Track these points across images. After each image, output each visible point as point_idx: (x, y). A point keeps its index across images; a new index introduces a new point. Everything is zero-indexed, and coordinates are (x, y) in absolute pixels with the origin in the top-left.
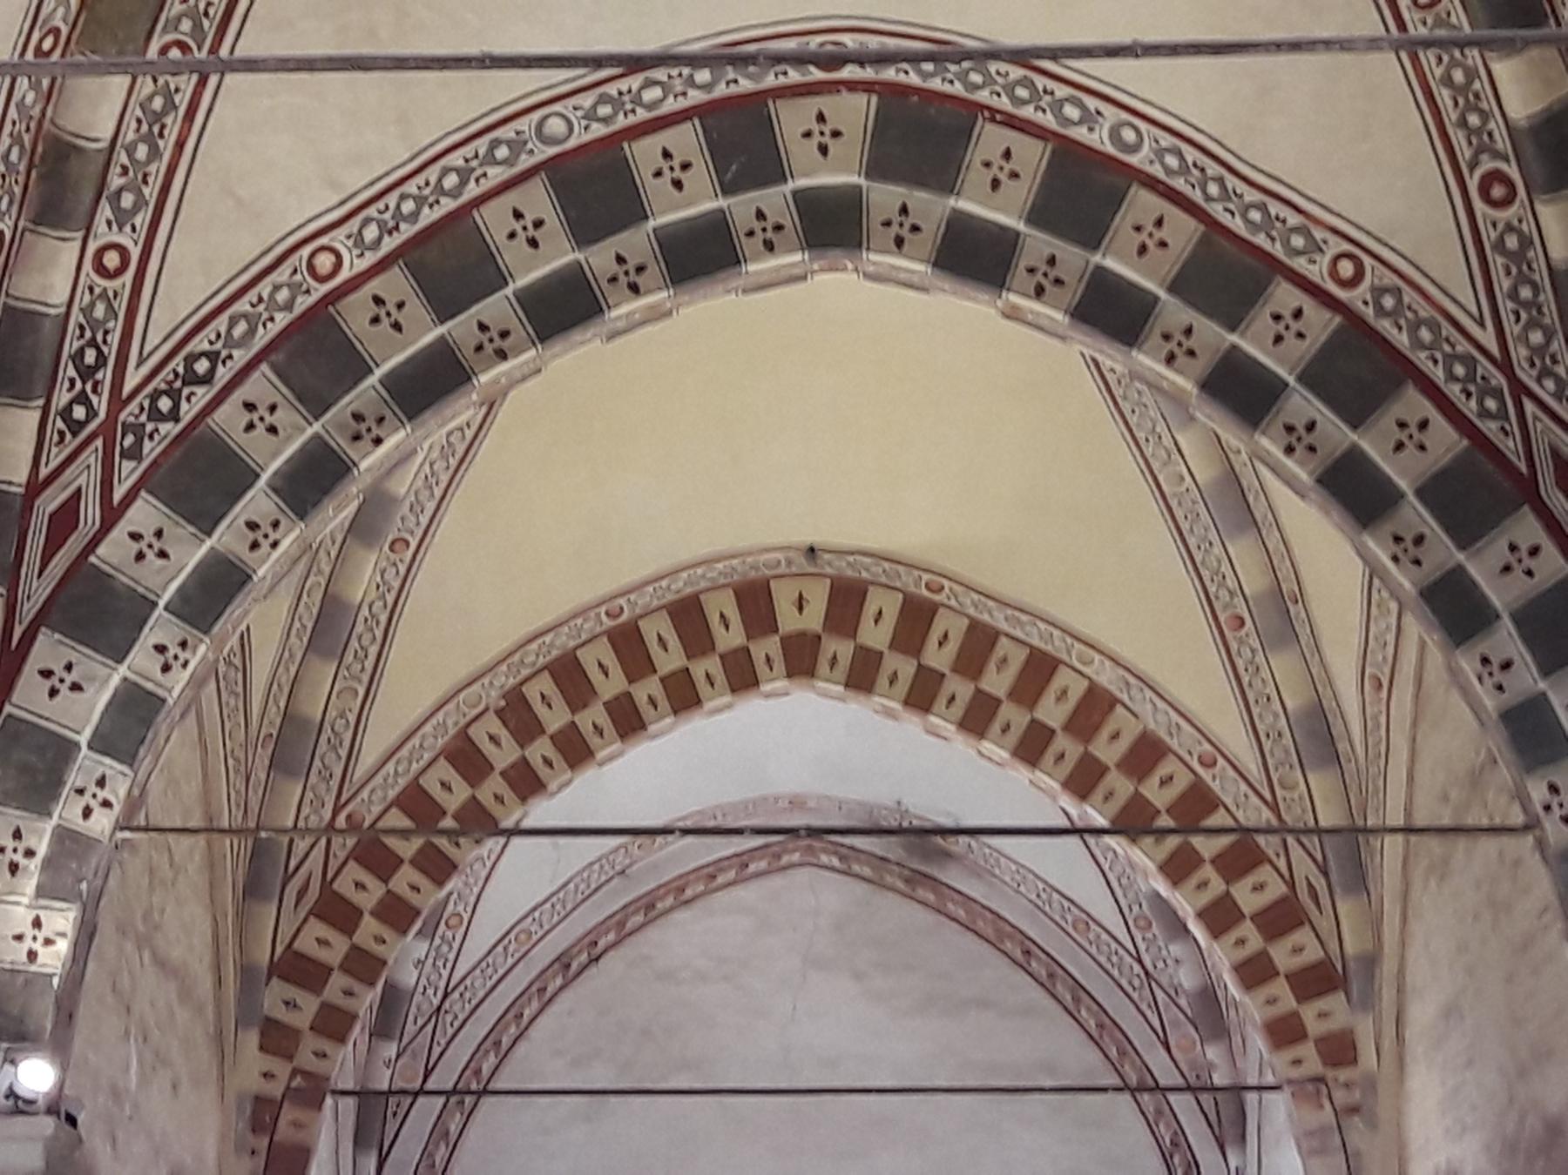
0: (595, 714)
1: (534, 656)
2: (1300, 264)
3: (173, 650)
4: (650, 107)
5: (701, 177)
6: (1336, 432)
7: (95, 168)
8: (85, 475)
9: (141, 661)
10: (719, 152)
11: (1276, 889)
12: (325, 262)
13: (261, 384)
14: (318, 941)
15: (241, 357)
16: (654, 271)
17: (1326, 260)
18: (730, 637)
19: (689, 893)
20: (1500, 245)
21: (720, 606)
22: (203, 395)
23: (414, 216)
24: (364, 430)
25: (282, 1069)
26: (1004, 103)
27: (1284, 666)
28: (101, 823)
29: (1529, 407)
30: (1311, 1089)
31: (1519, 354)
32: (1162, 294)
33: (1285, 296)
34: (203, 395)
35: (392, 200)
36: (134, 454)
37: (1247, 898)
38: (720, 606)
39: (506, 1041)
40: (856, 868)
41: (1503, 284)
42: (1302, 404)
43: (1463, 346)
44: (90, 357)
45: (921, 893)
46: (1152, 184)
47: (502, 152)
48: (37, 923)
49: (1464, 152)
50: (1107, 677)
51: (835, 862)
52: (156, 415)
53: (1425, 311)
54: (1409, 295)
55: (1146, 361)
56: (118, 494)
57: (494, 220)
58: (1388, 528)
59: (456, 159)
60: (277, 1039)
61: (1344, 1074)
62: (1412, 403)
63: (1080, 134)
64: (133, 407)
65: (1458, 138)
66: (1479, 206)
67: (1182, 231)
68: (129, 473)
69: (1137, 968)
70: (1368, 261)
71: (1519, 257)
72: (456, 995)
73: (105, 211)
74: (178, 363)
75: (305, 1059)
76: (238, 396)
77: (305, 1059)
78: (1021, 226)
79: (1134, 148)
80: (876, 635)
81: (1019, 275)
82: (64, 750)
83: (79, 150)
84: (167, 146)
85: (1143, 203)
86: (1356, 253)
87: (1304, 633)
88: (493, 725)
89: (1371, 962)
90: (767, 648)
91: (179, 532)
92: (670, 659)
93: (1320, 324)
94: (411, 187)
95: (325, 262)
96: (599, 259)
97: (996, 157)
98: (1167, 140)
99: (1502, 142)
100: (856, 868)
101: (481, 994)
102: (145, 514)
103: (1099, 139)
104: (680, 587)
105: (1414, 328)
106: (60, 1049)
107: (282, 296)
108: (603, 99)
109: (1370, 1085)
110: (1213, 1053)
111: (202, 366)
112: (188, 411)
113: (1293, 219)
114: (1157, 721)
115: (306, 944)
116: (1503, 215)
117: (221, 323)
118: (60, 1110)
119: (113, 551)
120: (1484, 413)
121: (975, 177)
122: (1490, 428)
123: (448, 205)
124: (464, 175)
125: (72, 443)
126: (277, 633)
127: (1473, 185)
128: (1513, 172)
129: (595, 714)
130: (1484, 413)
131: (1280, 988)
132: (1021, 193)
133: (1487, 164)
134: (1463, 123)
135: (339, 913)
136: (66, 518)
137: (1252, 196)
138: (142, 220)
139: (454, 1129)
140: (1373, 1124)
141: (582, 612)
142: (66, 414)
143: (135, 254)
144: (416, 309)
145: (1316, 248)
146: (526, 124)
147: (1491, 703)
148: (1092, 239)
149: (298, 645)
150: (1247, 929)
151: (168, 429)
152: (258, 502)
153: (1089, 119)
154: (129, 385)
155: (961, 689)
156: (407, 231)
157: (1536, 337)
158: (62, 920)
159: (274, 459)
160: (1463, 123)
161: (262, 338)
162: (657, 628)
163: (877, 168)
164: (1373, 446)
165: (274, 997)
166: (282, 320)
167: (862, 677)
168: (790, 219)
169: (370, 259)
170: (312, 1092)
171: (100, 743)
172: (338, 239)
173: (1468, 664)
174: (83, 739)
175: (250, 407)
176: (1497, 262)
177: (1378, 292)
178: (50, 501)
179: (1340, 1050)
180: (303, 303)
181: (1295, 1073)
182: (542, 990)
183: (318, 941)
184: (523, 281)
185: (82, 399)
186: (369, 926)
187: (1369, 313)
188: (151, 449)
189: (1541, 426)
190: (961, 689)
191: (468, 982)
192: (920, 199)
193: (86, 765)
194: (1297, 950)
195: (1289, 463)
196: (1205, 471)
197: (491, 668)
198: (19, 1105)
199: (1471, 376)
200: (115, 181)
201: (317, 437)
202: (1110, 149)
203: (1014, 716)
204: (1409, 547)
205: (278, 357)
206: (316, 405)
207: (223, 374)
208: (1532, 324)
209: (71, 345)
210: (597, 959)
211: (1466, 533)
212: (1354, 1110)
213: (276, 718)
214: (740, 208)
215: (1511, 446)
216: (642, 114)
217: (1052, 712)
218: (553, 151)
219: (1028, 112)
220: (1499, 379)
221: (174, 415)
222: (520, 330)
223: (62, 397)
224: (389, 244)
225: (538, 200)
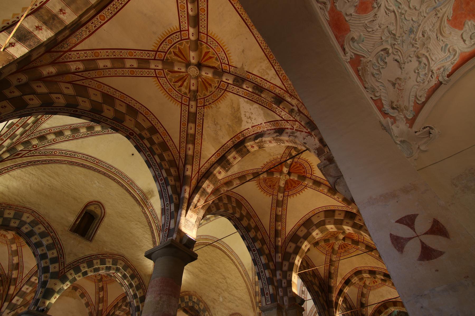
126: (251, 274)
213: (254, 281)
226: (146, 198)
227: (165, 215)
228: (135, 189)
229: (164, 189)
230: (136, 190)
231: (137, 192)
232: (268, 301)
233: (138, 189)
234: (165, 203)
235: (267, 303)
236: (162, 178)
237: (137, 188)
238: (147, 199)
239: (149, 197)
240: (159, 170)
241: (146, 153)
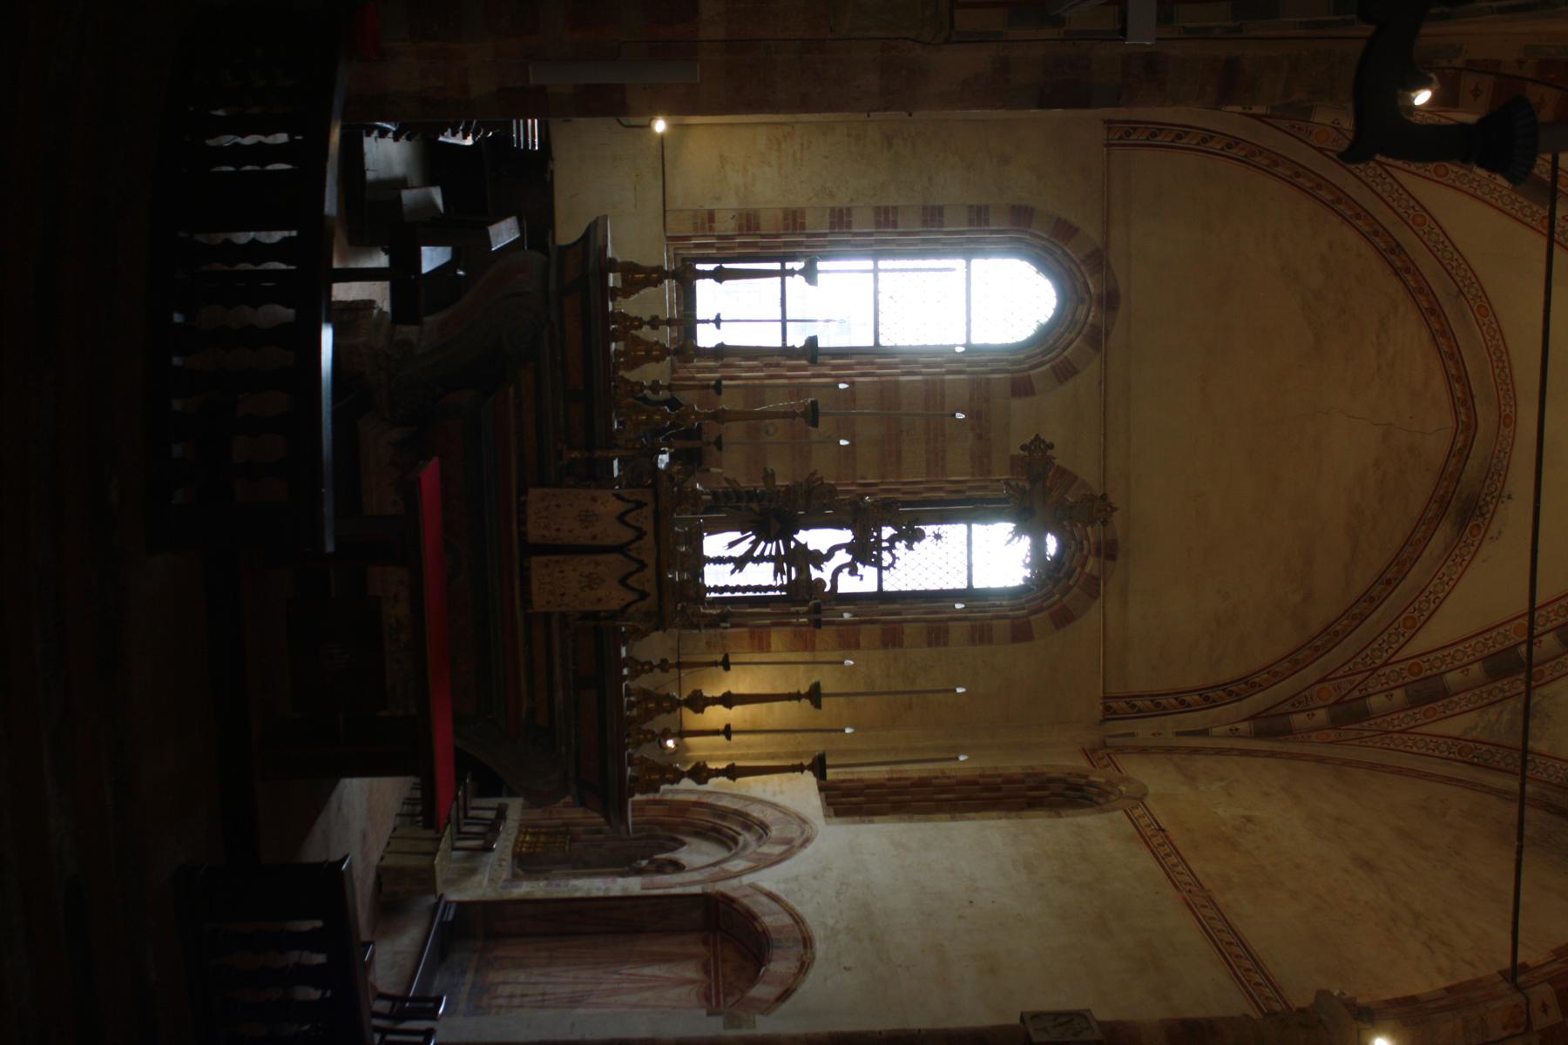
19: (1441, 340)
39: (1341, 207)
40: (1453, 461)
45: (1434, 506)
51: (1459, 445)
69: (1379, 662)
72: (1379, 171)
100: (1453, 461)
101: (1379, 189)
110: (1321, 715)
139: (1279, 170)
182: (1376, 233)
191: (1389, 180)
210: (1397, 274)
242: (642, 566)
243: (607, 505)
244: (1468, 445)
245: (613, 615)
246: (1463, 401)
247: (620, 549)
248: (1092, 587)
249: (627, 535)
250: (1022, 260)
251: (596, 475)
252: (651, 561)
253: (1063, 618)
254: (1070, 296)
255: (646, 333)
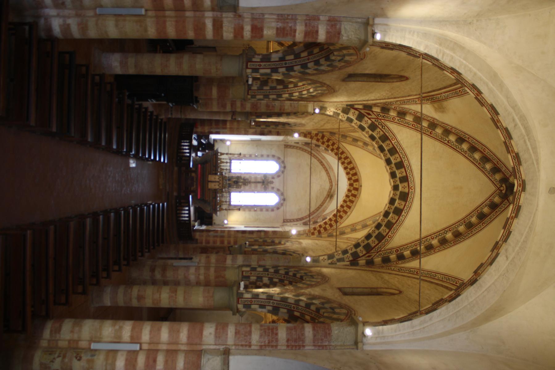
0: (346, 165)
1: (352, 159)
2: (390, 232)
3: (357, 124)
4: (408, 171)
5: (401, 175)
6: (374, 235)
7: (404, 118)
8: (373, 116)
9: (355, 121)
10: (403, 177)
11: (328, 229)
12: (393, 139)
13: (382, 133)
14: (325, 139)
15: (384, 131)
16: (391, 171)
17: (391, 235)
18: (353, 178)
20: (391, 251)
21: (356, 177)
22: (381, 127)
23: (397, 148)
24: (377, 143)
25: (314, 135)
26: (407, 205)
27: (349, 230)
28: (340, 117)
29: (376, 253)
30: (309, 231)
31: (381, 252)
32: (388, 219)
33: (387, 231)
34: (381, 127)
35: (399, 146)
36: (375, 121)
37: (327, 226)
38: (356, 177)
41: (388, 251)
42: (377, 232)
43: (382, 247)
44: (385, 117)
45: (327, 196)
46: (398, 219)
47: (403, 156)
48: (331, 111)
49: (401, 248)
50: (348, 214)
52: (379, 123)
53: (385, 244)
54: (387, 242)
55: (382, 217)
56: (371, 119)
57: (397, 155)
58: (365, 239)
59: (403, 152)
60: (317, 135)
61: (311, 234)
62: (377, 242)
63: (404, 212)
64: (380, 121)
65: (402, 247)
66: (395, 249)
67: (394, 221)
68: (373, 120)
70: (390, 239)
71: (390, 252)
73: (399, 118)
74: (384, 125)
75: (315, 137)
76: (381, 131)
77: (315, 137)
78: (395, 206)
79: (402, 217)
80: (353, 192)
81: (390, 205)
82: (347, 114)
83: (405, 116)
84: (405, 124)
85: (397, 217)
86: (391, 238)
87: (352, 232)
88: (345, 155)
89: (321, 237)
90: (352, 182)
91: (368, 125)
92: (351, 172)
93: (385, 234)
94: (400, 148)
95: (393, 139)
96: (393, 165)
97: (402, 204)
98: (403, 220)
99: (401, 252)
102: (370, 122)
103: (403, 213)
104: (358, 173)
105: (384, 243)
106: (319, 113)
107: (390, 135)
108: (408, 166)
109: (310, 236)
111: (384, 127)
112: (379, 126)
113: (395, 232)
114: (344, 218)
115: (325, 138)
116: (395, 252)
117: (388, 129)
118: (314, 113)
119: (366, 119)
120: (375, 249)
121: (400, 202)
122: (374, 249)
123: (398, 151)
124: (402, 153)
125: (376, 115)
127: (398, 249)
128: (399, 252)
129: (346, 165)
130: (375, 249)
131: (319, 229)
132: (398, 206)
133: (399, 250)
134: (403, 248)
135: (328, 141)
136: (369, 114)
137: (397, 228)
138: (398, 122)
140: (306, 237)
141: (356, 164)
142: (379, 114)
143: (395, 121)
144: (389, 148)
145: (392, 234)
146: (406, 159)
147: (348, 248)
148: (394, 212)
149: (354, 137)
150: (324, 226)
151: (378, 124)
152: (371, 132)
153: (405, 213)
154: (382, 121)
155: (348, 200)
156: (396, 147)
157: (383, 254)
158: (331, 114)
159: (374, 134)
160: (403, 248)
161: (386, 133)
162: (354, 171)
163: (401, 192)
164: (373, 238)
165: (320, 135)
166: (388, 135)
167: (349, 191)
168: (396, 184)
169: (394, 144)
170: (312, 138)
171: (348, 118)
172: (396, 140)
173: (352, 246)
174: (348, 116)
175: (380, 132)
176: (390, 251)
177: (388, 240)
178: (371, 113)
179: (313, 234)
180: (389, 137)
181: (311, 230)
183: (325, 139)
184: (391, 158)
185: (381, 116)
186: (327, 143)
187: (385, 238)
188: (376, 122)
189: (374, 254)
190: (348, 200)
192: (398, 196)
193: (346, 116)
194: (322, 230)
195: (372, 230)
196: (368, 223)
197: (351, 155)
198: (314, 110)
199: (379, 248)
200: (402, 119)
201: (376, 138)
202: (402, 214)
203: (345, 205)
204: (363, 241)
205: (384, 135)
206: (380, 138)
207: (383, 129)
208: (384, 254)
209: (386, 115)
211: (364, 247)
212: (307, 235)
214: (398, 179)
215: (372, 251)
216: (407, 170)
217: (345, 208)
218: (404, 161)
219: (406, 207)
220: (379, 250)
221: (379, 124)
222: (387, 158)
223: (381, 114)
224: (395, 145)
225: (399, 160)
226: (434, 100)
227: (266, 299)
228: (448, 93)
229: (287, 306)
230: (446, 94)
231: (444, 94)
232: (246, 273)
233: (448, 97)
234: (277, 302)
235: (244, 272)
236: (295, 310)
237: (450, 97)
238: (432, 101)
239: (436, 105)
240: (301, 311)
241: (314, 314)
242: (220, 184)
243: (217, 177)
244: (332, 188)
245: (217, 189)
246: (331, 182)
247: (218, 182)
248: (282, 205)
249: (218, 180)
250: (277, 163)
251: (216, 174)
252: (221, 183)
253: (278, 208)
254: (280, 167)
255: (222, 160)
